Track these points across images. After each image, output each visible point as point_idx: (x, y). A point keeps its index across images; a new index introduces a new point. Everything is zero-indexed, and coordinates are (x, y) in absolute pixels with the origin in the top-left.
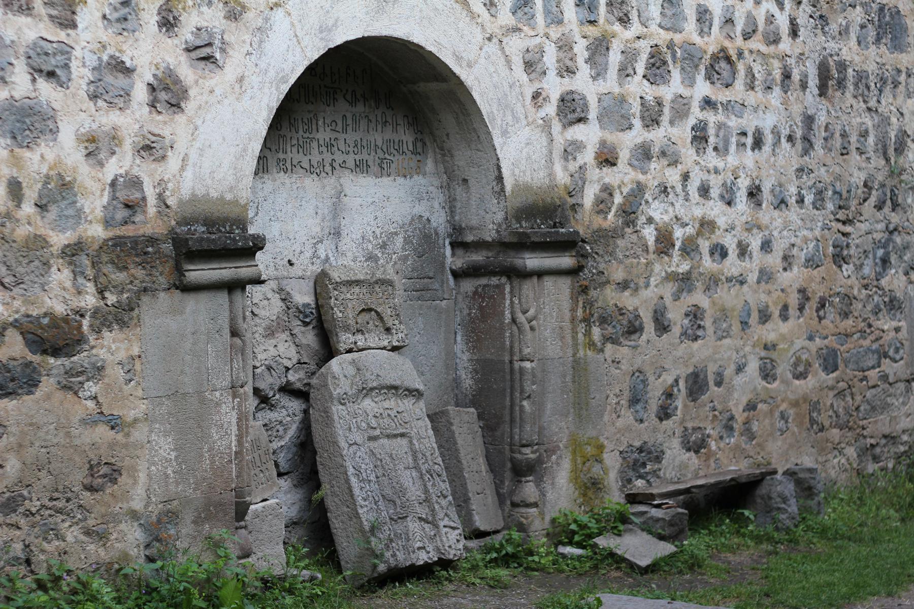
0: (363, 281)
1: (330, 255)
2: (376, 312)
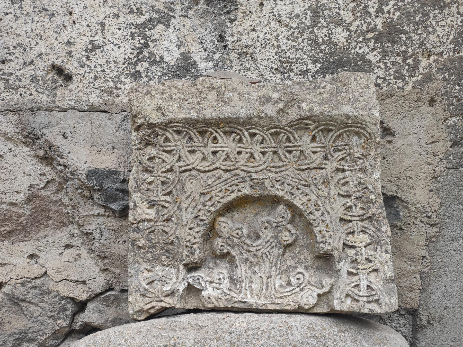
0: (248, 122)
1: (198, 55)
2: (290, 206)
